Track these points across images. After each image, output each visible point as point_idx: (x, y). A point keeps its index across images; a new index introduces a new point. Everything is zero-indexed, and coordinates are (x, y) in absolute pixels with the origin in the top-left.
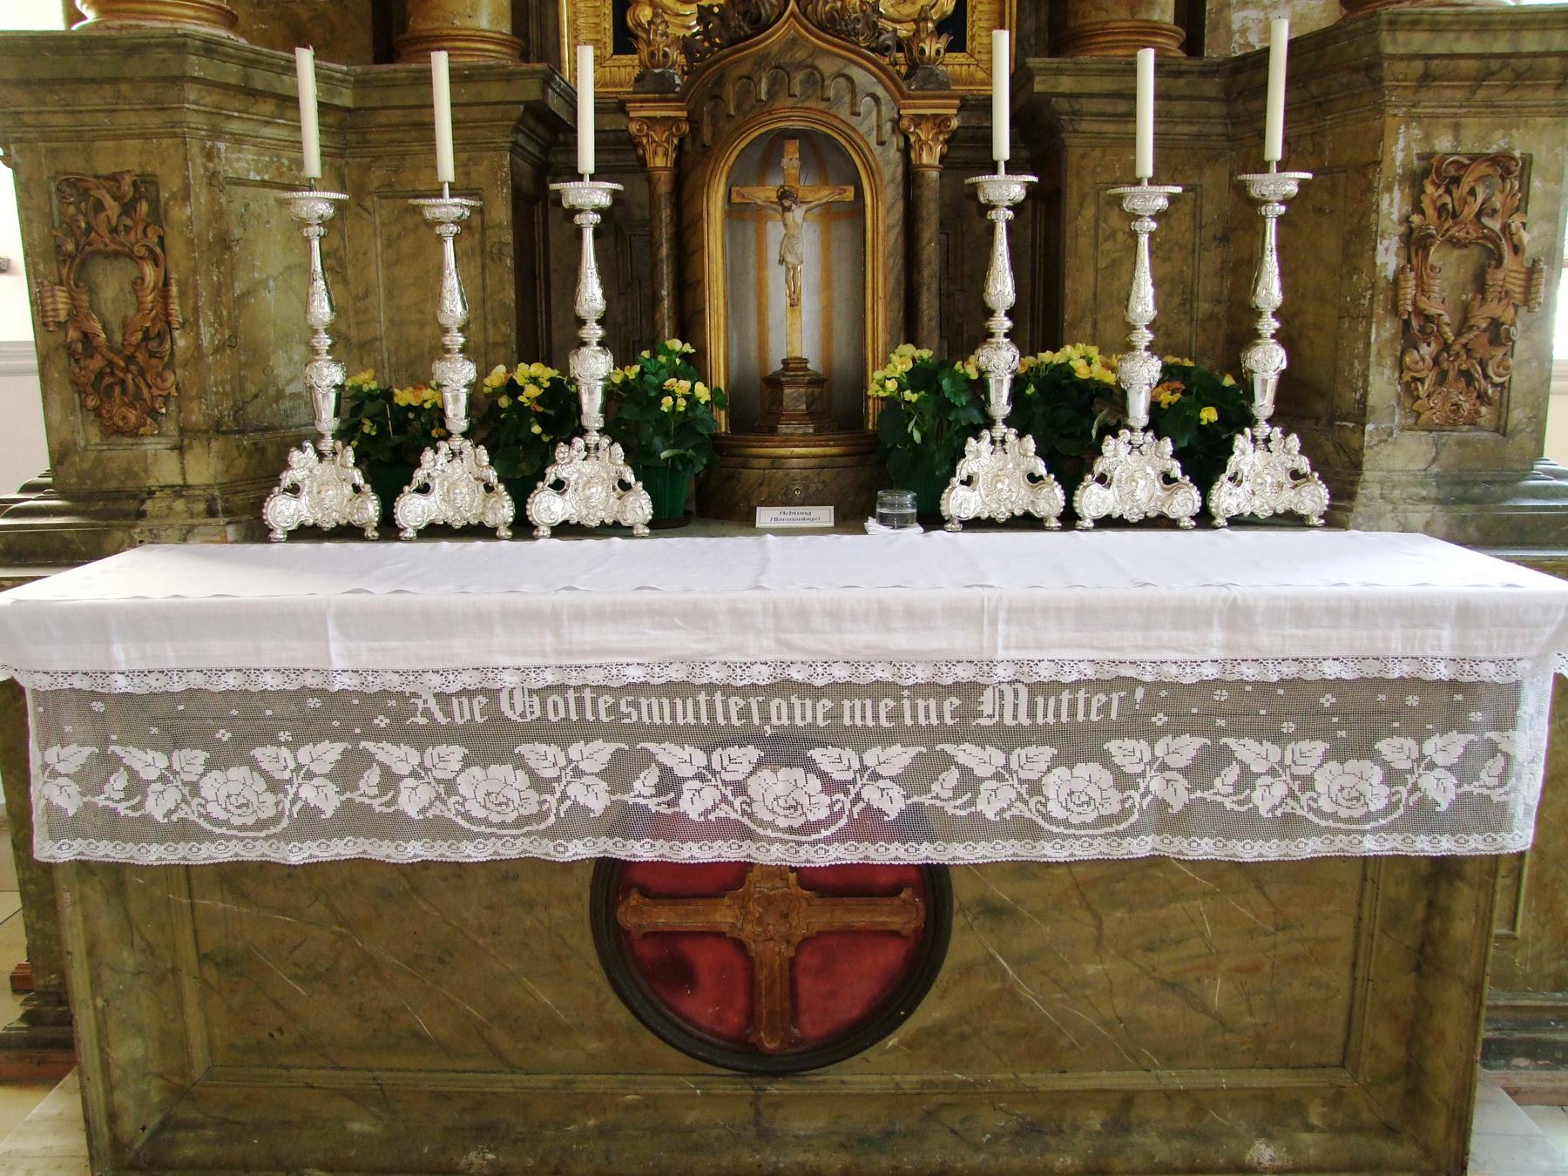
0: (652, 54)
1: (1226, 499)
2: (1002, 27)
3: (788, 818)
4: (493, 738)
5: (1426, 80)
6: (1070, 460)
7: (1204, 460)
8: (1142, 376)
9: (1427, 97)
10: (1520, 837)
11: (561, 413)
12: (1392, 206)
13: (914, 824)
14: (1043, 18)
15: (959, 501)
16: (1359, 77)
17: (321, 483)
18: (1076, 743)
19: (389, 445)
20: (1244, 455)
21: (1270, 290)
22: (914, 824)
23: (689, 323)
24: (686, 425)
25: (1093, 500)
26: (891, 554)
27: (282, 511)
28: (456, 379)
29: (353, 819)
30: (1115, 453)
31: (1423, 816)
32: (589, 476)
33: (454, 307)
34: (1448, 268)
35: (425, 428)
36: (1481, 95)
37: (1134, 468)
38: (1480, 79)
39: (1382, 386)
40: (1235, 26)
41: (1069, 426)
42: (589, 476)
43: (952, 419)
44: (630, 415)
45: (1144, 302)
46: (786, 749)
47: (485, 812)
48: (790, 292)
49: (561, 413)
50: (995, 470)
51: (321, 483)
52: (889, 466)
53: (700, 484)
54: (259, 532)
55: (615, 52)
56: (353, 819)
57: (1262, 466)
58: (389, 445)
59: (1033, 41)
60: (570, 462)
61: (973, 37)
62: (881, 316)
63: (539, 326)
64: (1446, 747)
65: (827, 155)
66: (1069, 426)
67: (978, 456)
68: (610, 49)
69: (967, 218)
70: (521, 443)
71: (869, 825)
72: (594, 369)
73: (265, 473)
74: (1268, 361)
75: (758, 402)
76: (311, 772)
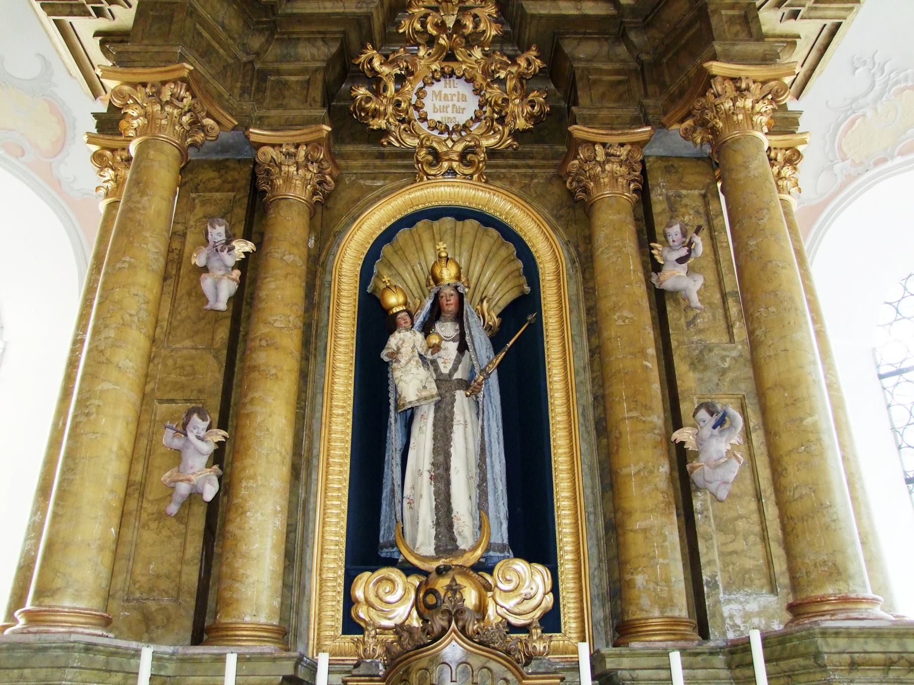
0: (365, 650)
2: (584, 640)
5: (853, 665)
9: (856, 675)
14: (608, 611)
16: (811, 662)
36: (892, 675)
38: (888, 665)
40: (726, 614)
55: (344, 633)
59: (602, 624)
61: (565, 623)
68: (340, 632)
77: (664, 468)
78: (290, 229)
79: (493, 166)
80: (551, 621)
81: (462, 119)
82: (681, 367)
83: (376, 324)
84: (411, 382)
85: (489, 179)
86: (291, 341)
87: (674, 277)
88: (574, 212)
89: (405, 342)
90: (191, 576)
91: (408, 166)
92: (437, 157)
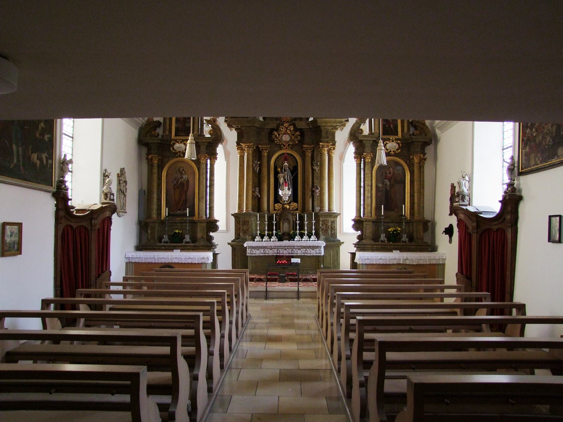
1: (311, 239)
3: (285, 253)
4: (271, 249)
6: (302, 237)
7: (310, 237)
8: (306, 232)
10: (323, 254)
11: (272, 235)
12: (321, 222)
13: (291, 253)
15: (295, 240)
17: (258, 238)
18: (299, 249)
19: (262, 236)
20: (312, 237)
21: (314, 227)
22: (291, 253)
23: (280, 229)
24: (280, 235)
25: (303, 239)
26: (291, 243)
27: (256, 240)
28: (266, 232)
29: (264, 253)
30: (304, 237)
31: (317, 253)
32: (274, 238)
33: (266, 228)
34: (324, 226)
35: (264, 235)
37: (305, 238)
39: (321, 233)
41: (302, 235)
42: (274, 238)
43: (295, 235)
44: (276, 235)
45: (306, 228)
46: (285, 250)
47: (270, 253)
48: (285, 227)
49: (272, 235)
50: (297, 238)
51: (258, 238)
52: (291, 238)
53: (280, 239)
54: (254, 241)
56: (264, 253)
57: (313, 238)
58: (262, 236)
60: (273, 237)
62: (291, 229)
63: (270, 229)
64: (318, 250)
65: (288, 220)
66: (302, 235)
67: (296, 237)
69: (296, 223)
70: (270, 236)
71: (289, 253)
72: (274, 232)
73: (255, 238)
74: (314, 232)
75: (284, 234)
76: (262, 251)
77: (310, 193)
78: (265, 160)
79: (292, 147)
80: (297, 209)
81: (288, 140)
82: (315, 179)
83: (276, 173)
84: (281, 180)
85: (292, 149)
86: (266, 177)
87: (315, 168)
88: (303, 155)
89: (280, 175)
90: (257, 205)
91: (280, 147)
92: (284, 145)
